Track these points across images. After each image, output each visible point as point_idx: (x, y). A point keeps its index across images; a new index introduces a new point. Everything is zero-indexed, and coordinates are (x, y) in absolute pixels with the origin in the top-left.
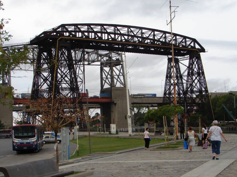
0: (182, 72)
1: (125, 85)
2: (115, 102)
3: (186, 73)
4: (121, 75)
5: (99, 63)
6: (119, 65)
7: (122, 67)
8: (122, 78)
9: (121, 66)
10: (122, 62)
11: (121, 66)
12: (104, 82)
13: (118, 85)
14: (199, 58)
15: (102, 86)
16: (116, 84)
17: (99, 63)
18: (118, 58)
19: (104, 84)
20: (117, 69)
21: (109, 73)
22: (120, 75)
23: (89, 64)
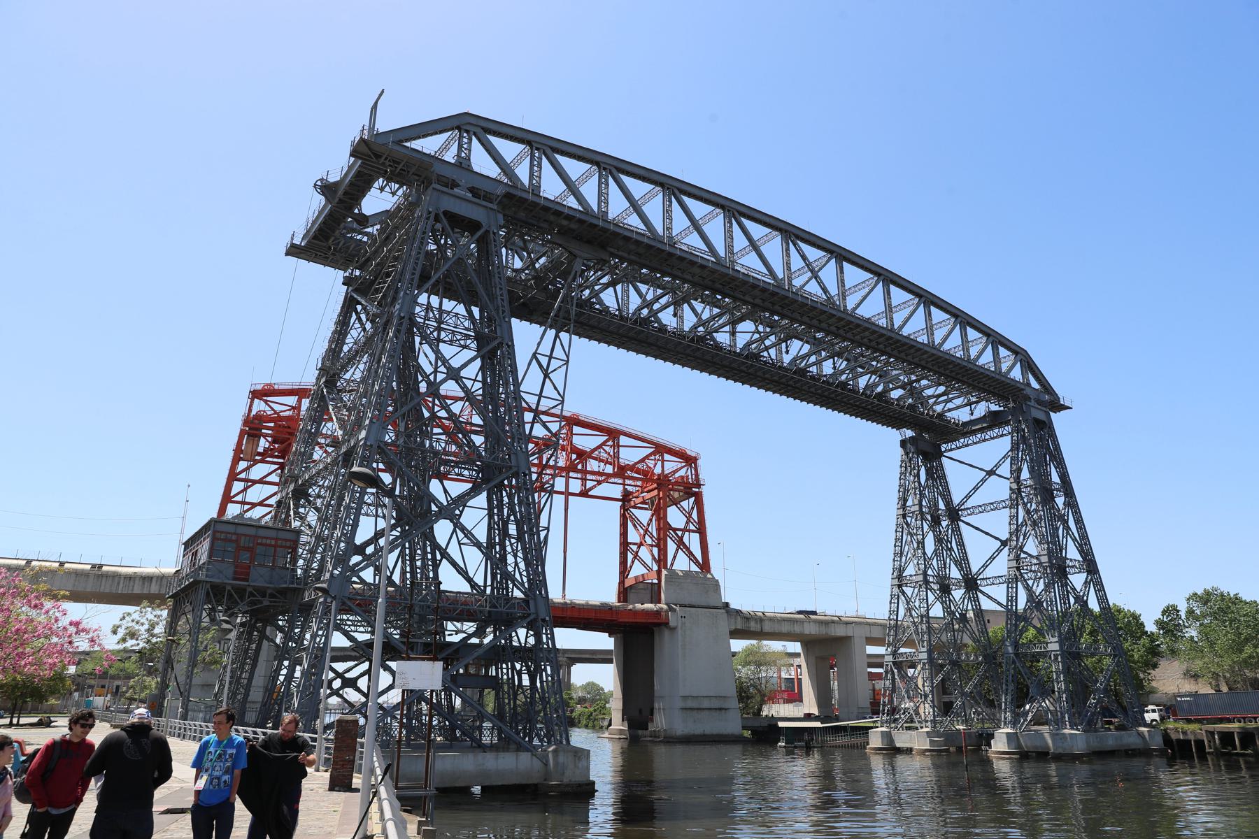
0: (956, 500)
1: (705, 566)
2: (672, 624)
3: (999, 489)
4: (693, 531)
5: (615, 490)
6: (688, 498)
7: (699, 503)
8: (693, 541)
9: (692, 500)
10: (699, 486)
11: (692, 500)
12: (630, 557)
13: (682, 564)
14: (1044, 429)
15: (624, 569)
16: (672, 564)
17: (615, 490)
18: (682, 473)
19: (633, 562)
20: (682, 510)
21: (650, 529)
22: (689, 531)
23: (584, 494)
